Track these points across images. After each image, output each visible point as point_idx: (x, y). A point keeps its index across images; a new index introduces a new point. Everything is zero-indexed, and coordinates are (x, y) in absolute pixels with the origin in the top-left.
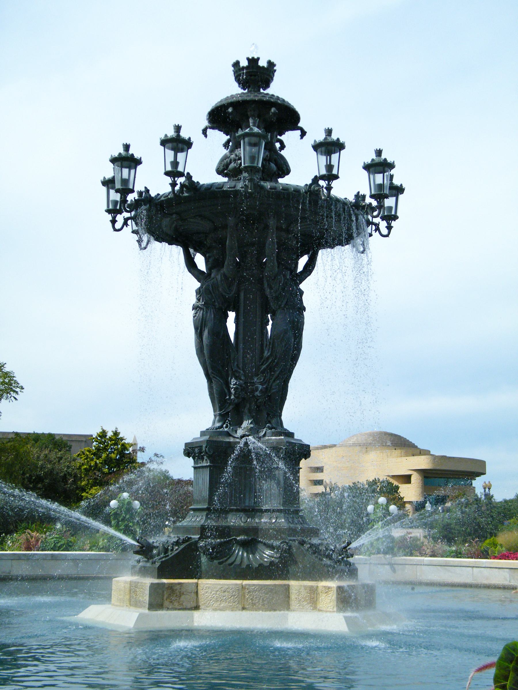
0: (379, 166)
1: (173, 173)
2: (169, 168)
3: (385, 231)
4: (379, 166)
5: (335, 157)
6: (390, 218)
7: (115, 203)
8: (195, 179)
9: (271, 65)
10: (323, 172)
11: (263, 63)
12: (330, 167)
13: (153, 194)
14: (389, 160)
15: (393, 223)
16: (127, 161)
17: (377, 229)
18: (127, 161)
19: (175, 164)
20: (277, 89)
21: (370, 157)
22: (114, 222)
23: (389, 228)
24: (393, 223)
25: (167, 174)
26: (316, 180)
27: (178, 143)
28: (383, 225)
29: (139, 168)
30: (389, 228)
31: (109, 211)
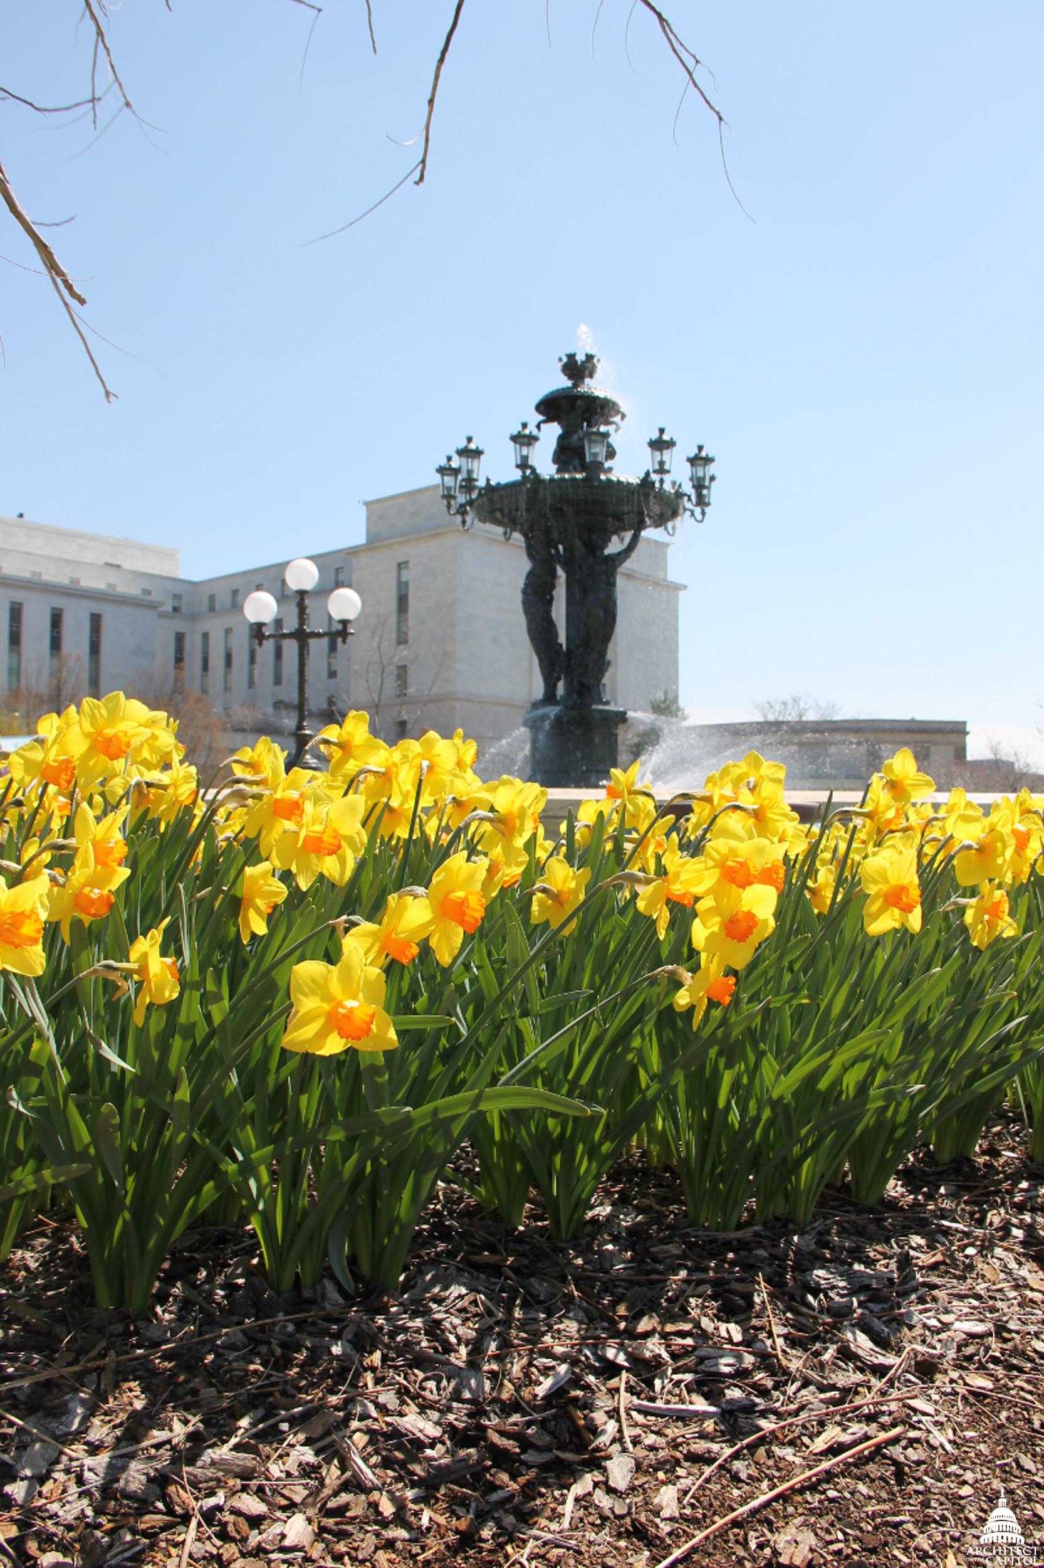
0: (699, 460)
1: (523, 465)
2: (519, 462)
3: (699, 517)
4: (699, 460)
5: (667, 455)
6: (702, 502)
7: (449, 489)
8: (538, 471)
9: (590, 358)
10: (657, 467)
11: (580, 358)
12: (662, 463)
13: (493, 483)
14: (710, 456)
15: (707, 510)
16: (470, 453)
17: (693, 514)
18: (470, 453)
19: (525, 459)
20: (597, 386)
21: (693, 452)
22: (449, 506)
23: (703, 513)
24: (707, 510)
25: (518, 466)
26: (648, 474)
27: (523, 439)
28: (698, 510)
29: (482, 457)
30: (703, 513)
31: (444, 497)
